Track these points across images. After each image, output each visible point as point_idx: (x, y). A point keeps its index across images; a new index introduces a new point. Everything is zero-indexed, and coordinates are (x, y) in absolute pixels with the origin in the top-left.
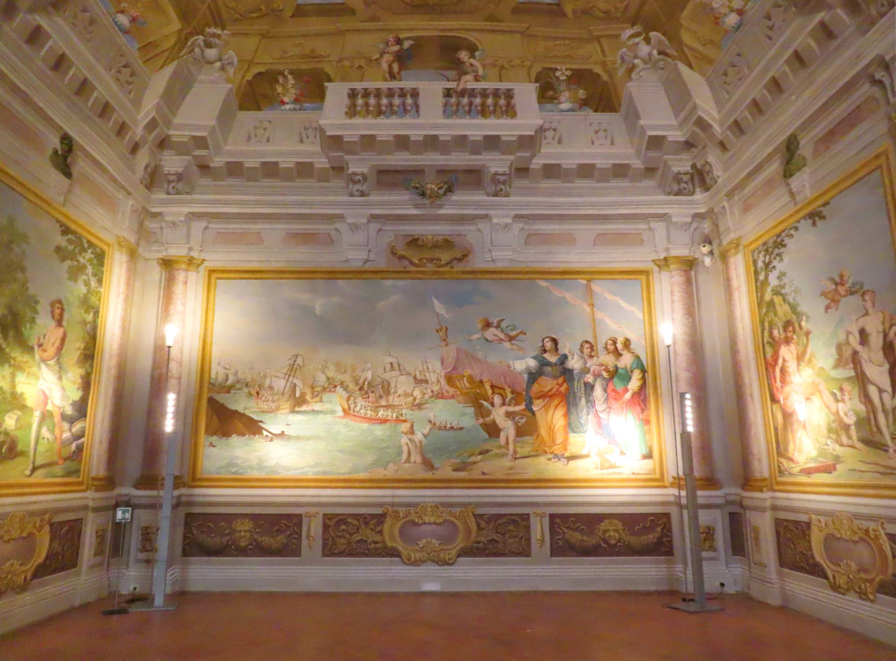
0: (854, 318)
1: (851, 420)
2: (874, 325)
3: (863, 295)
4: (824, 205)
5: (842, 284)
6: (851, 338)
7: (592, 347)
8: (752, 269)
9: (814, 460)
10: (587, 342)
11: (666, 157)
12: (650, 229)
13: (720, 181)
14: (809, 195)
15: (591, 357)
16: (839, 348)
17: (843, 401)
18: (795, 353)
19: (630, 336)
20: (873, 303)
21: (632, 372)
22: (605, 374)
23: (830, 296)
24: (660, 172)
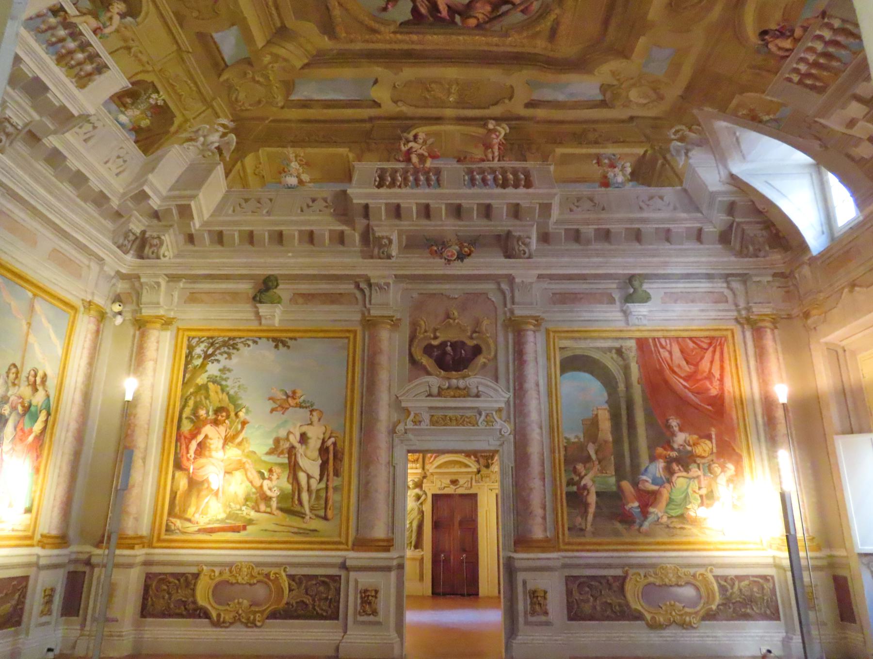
0: (299, 425)
1: (274, 494)
2: (315, 434)
3: (311, 411)
4: (291, 339)
5: (294, 398)
6: (291, 437)
7: (17, 373)
8: (185, 351)
9: (222, 521)
10: (15, 366)
11: (135, 212)
12: (89, 267)
14: (277, 325)
15: (14, 384)
16: (277, 441)
17: (270, 479)
18: (223, 435)
19: (49, 373)
20: (319, 420)
22: (20, 408)
23: (278, 402)
24: (123, 220)
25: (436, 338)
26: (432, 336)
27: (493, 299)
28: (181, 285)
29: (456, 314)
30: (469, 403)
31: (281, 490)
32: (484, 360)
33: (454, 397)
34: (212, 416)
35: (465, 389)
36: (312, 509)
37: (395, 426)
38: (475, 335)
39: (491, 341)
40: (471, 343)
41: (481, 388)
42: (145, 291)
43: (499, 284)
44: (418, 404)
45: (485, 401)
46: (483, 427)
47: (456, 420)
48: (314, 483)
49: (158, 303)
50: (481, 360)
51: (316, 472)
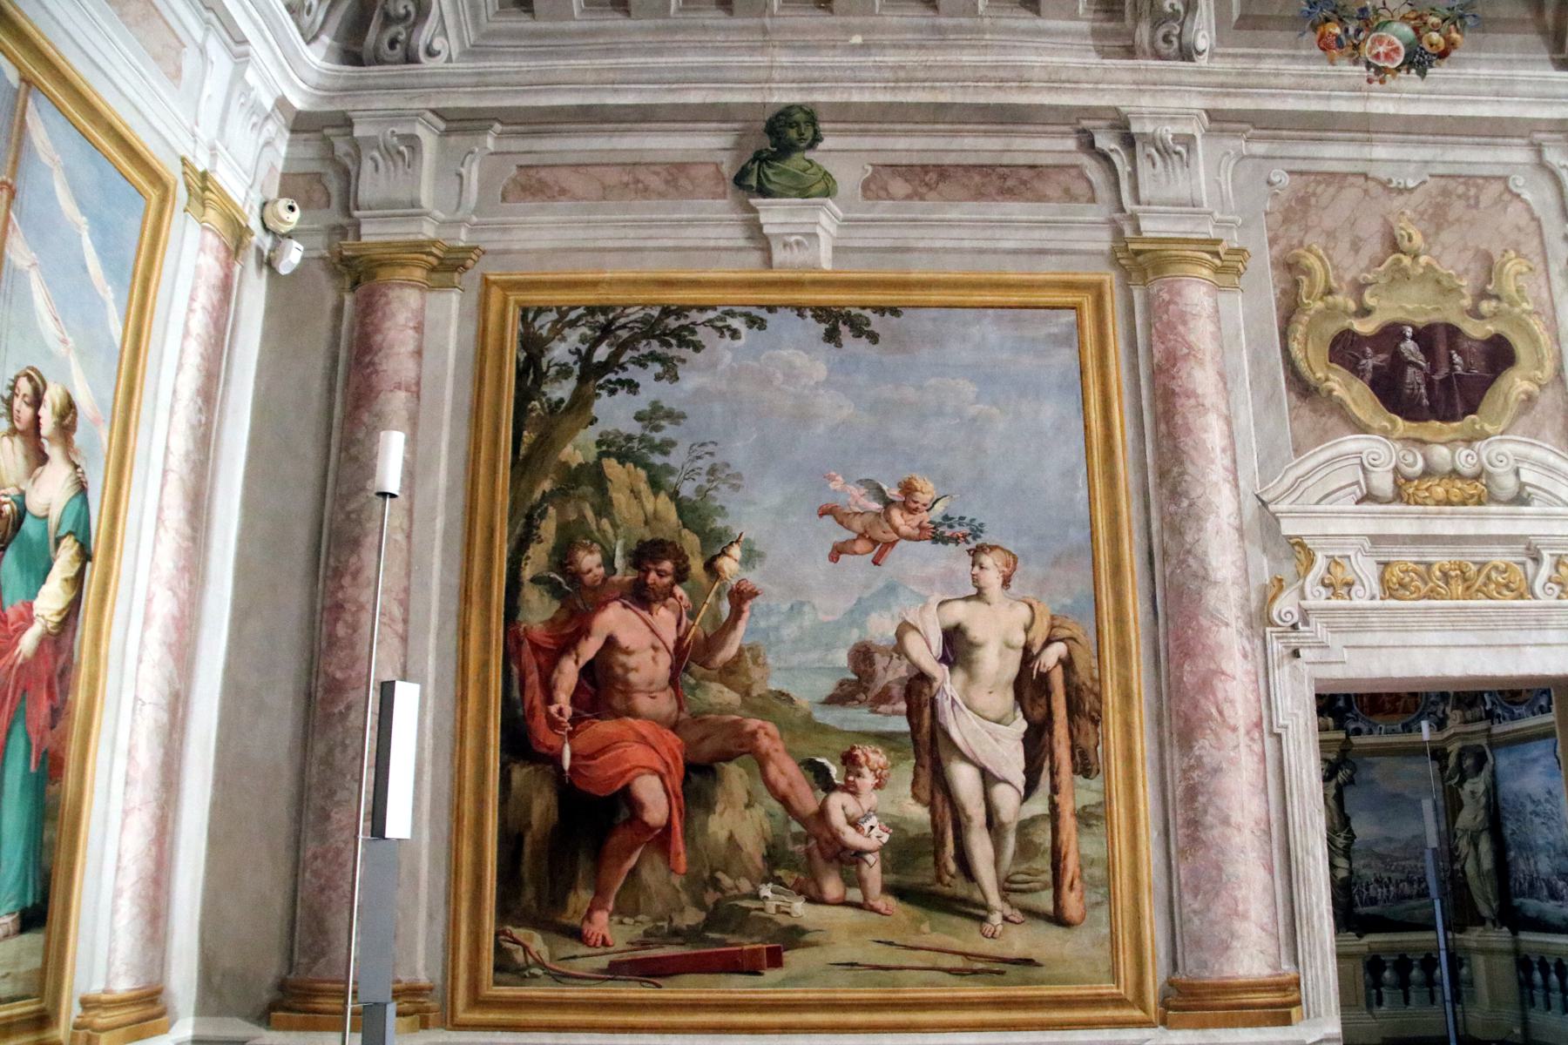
0: (936, 598)
2: (999, 630)
3: (976, 553)
4: (880, 310)
5: (908, 508)
6: (914, 644)
8: (513, 354)
13: (427, 64)
14: (827, 265)
17: (851, 789)
18: (670, 637)
19: (83, 399)
20: (1006, 583)
21: (58, 542)
23: (857, 524)
25: (1364, 312)
26: (1352, 306)
27: (1527, 195)
28: (490, 142)
29: (1418, 239)
30: (1496, 521)
31: (895, 826)
32: (1526, 386)
33: (1449, 503)
34: (623, 572)
35: (1477, 477)
36: (1007, 888)
37: (1268, 598)
38: (1486, 306)
39: (1537, 326)
40: (1477, 330)
41: (1527, 476)
42: (367, 166)
43: (1538, 149)
44: (1333, 528)
45: (1548, 517)
46: (1553, 602)
47: (1464, 577)
48: (1007, 799)
49: (414, 203)
50: (1516, 383)
51: (1009, 758)
